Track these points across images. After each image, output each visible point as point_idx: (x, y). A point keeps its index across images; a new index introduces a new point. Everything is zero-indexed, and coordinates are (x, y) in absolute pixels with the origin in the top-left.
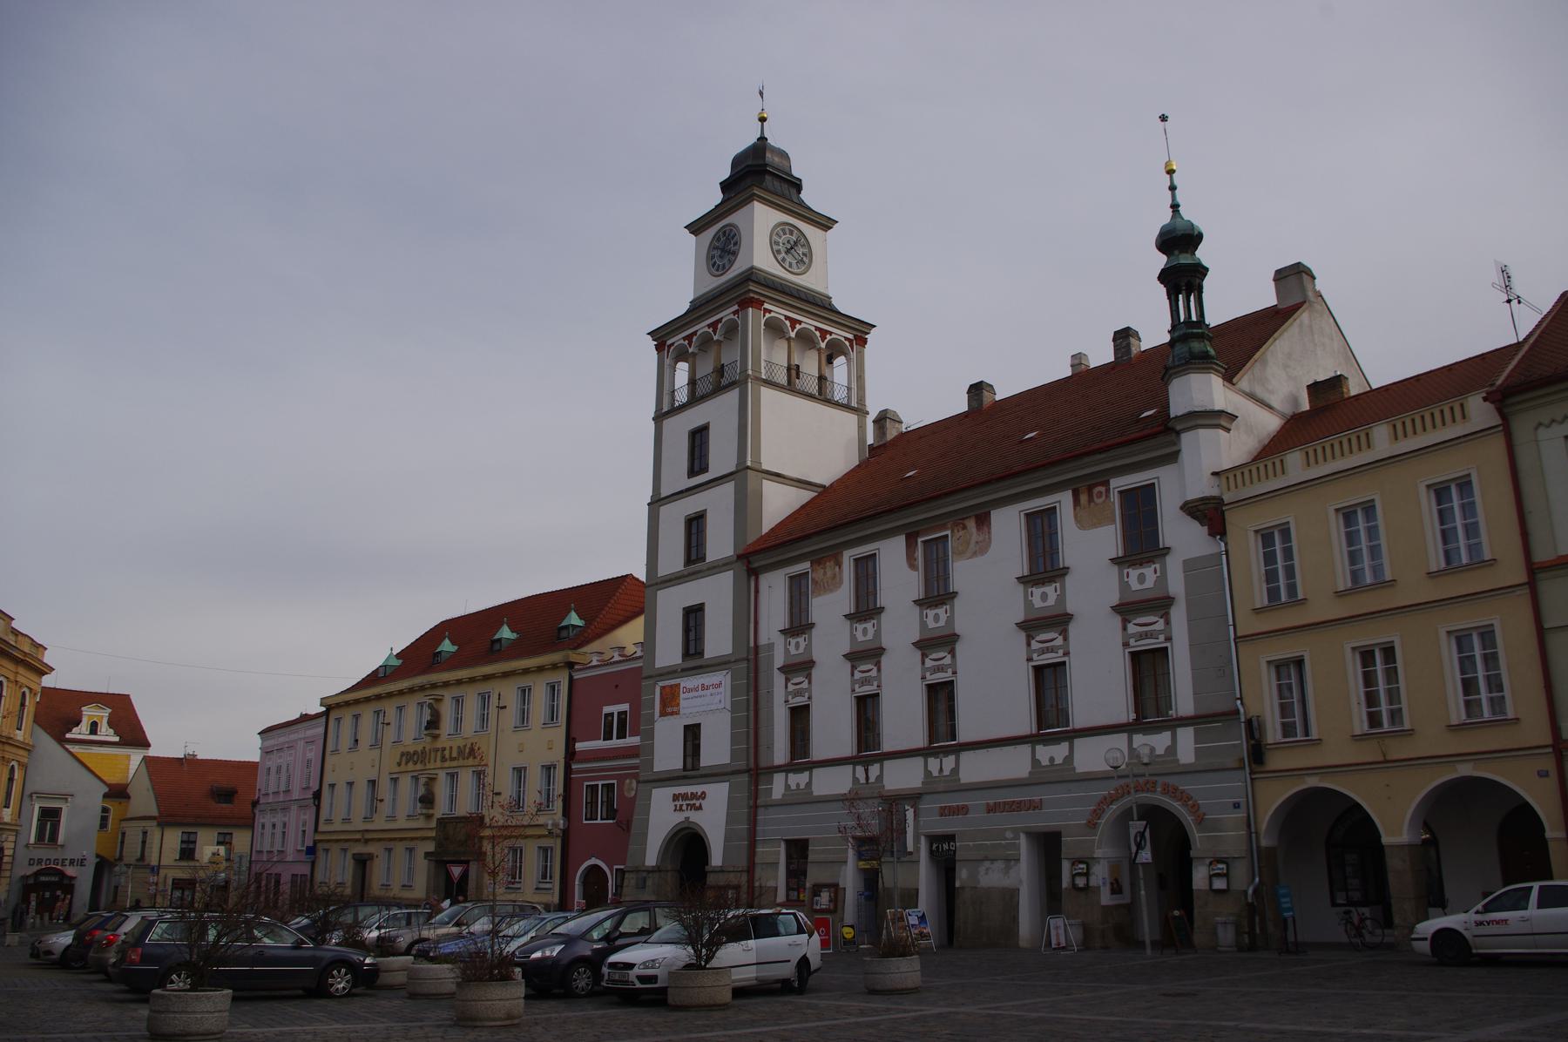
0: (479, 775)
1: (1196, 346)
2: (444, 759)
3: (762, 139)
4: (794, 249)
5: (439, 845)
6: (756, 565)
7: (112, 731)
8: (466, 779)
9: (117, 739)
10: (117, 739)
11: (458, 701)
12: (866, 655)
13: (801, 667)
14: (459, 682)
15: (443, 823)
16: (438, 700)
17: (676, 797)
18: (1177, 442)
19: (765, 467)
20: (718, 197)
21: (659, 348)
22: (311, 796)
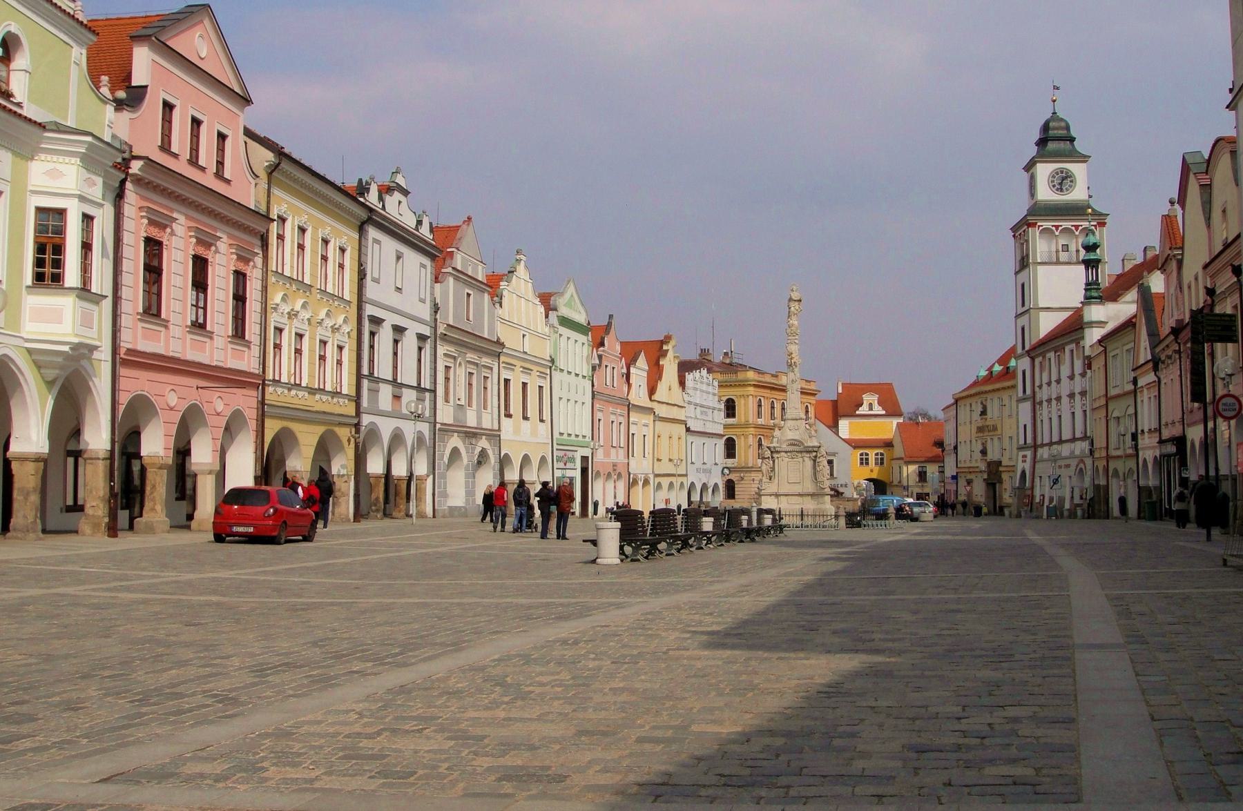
0: (999, 438)
1: (1088, 293)
2: (989, 431)
3: (1054, 113)
4: (1063, 181)
5: (988, 475)
6: (1033, 355)
7: (880, 408)
8: (996, 439)
9: (884, 412)
10: (884, 412)
11: (992, 399)
12: (1049, 401)
13: (1041, 403)
14: (990, 391)
15: (990, 464)
16: (986, 400)
17: (1024, 456)
18: (1083, 333)
19: (1040, 306)
20: (1033, 150)
21: (1014, 236)
22: (952, 448)
